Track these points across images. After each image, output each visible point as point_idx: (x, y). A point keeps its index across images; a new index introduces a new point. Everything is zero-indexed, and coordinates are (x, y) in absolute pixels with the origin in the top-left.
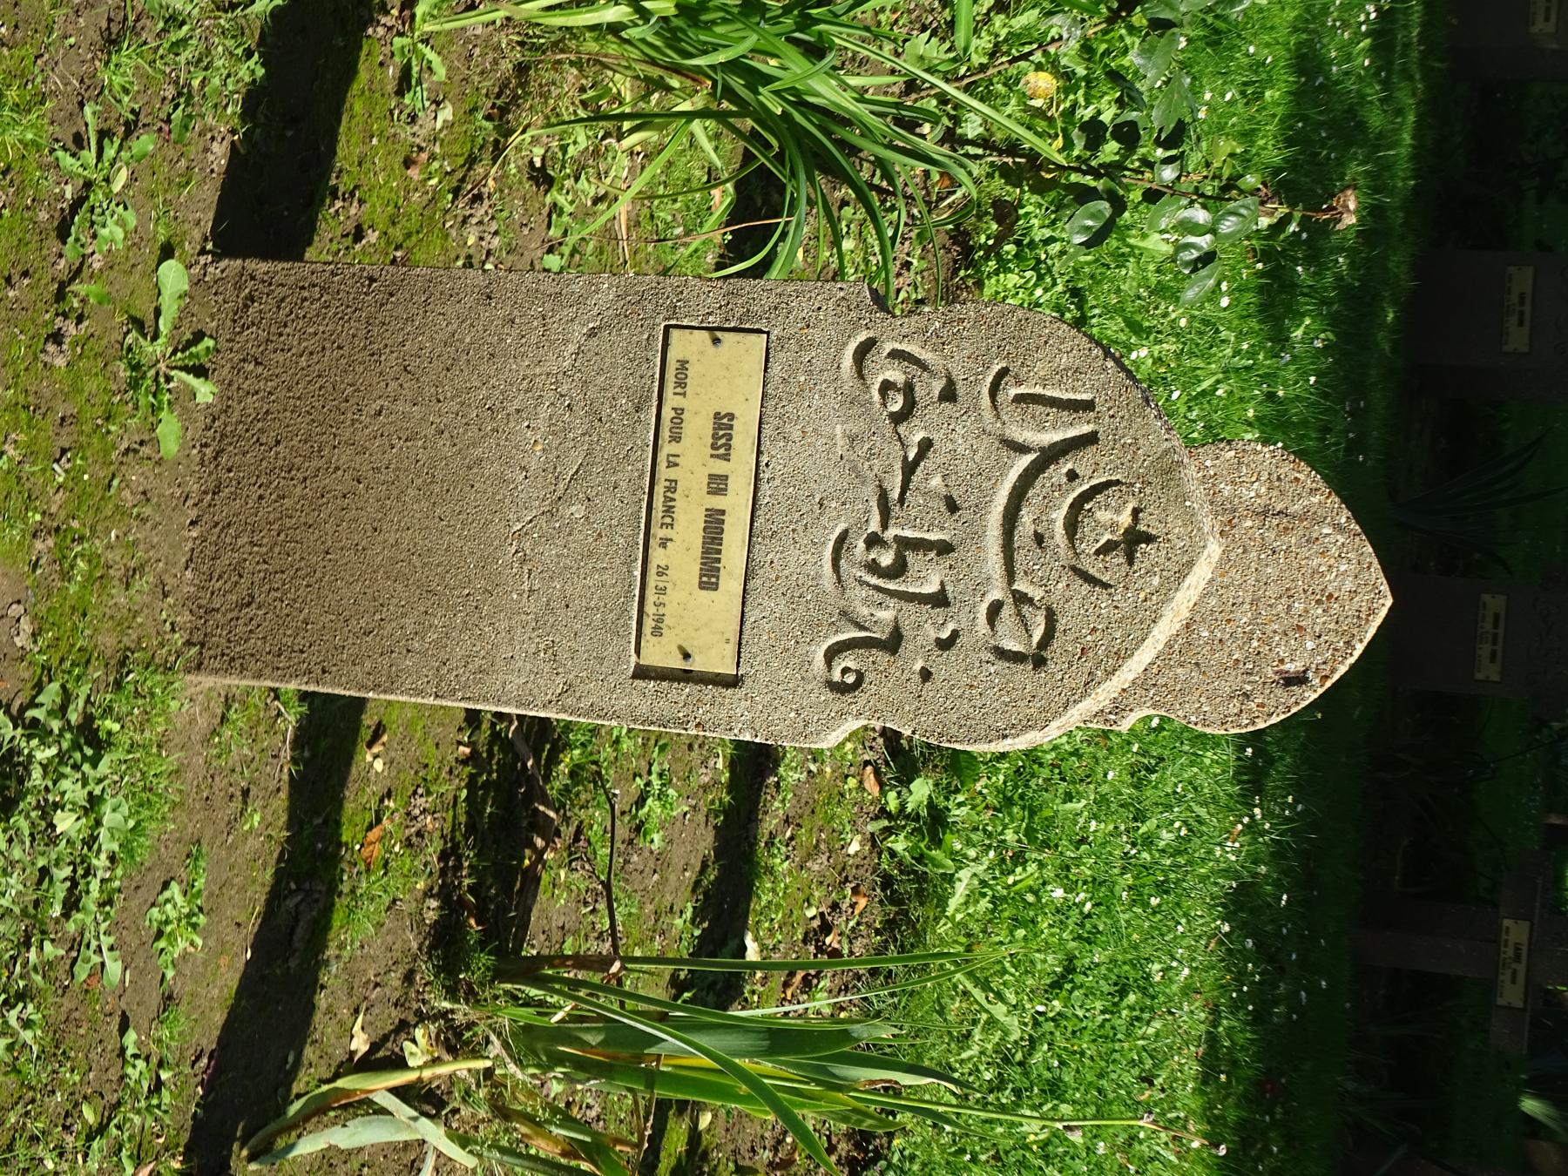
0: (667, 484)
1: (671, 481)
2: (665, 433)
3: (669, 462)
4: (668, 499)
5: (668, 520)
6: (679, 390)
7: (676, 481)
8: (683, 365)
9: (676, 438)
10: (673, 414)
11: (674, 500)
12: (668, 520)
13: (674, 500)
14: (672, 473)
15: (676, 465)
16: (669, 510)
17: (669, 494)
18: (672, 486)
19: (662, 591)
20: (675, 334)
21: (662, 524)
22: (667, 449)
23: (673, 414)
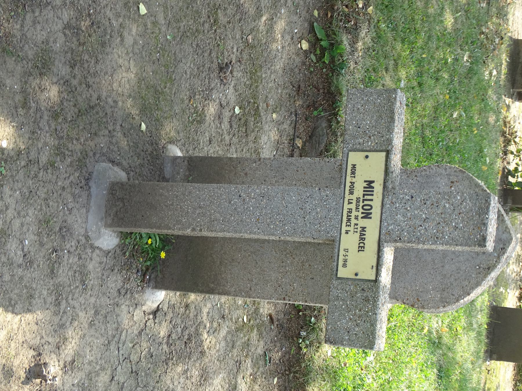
0: (348, 210)
1: (350, 209)
2: (347, 192)
3: (349, 202)
4: (348, 216)
5: (348, 224)
6: (352, 175)
7: (352, 209)
8: (354, 166)
9: (351, 193)
10: (350, 184)
11: (351, 216)
12: (348, 224)
13: (351, 216)
15: (352, 203)
16: (349, 220)
18: (350, 211)
19: (346, 250)
21: (346, 225)
22: (347, 197)
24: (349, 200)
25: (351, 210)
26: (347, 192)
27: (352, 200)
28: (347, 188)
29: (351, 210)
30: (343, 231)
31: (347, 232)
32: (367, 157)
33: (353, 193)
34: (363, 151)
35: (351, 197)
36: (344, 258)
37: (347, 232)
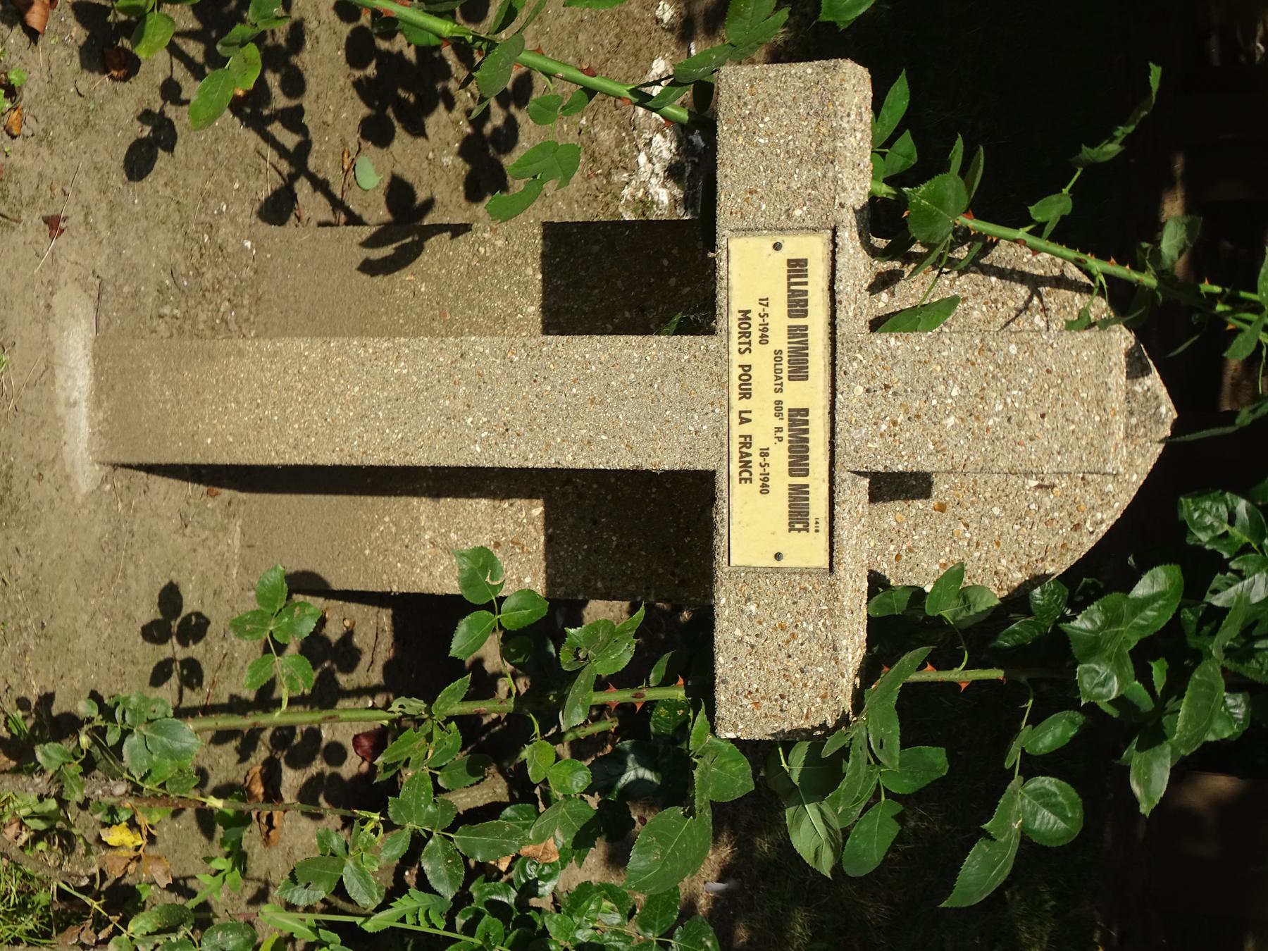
0: (742, 440)
1: (746, 437)
3: (741, 418)
4: (743, 455)
5: (745, 475)
7: (750, 437)
10: (740, 371)
12: (745, 475)
14: (746, 429)
15: (749, 420)
16: (746, 466)
17: (744, 450)
18: (746, 442)
21: (741, 480)
22: (738, 404)
23: (740, 371)
24: (741, 412)
25: (748, 439)
26: (735, 392)
27: (750, 412)
28: (735, 382)
29: (748, 439)
33: (750, 394)
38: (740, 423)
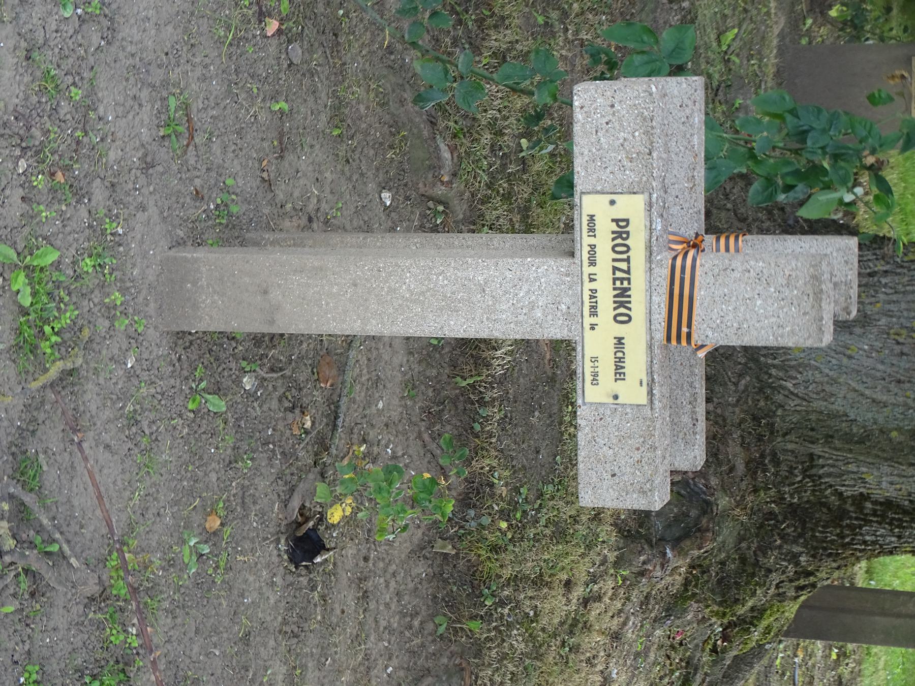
6: (591, 234)
9: (592, 263)
10: (589, 249)
14: (593, 285)
15: (595, 280)
19: (594, 360)
20: (584, 197)
22: (587, 270)
24: (590, 274)
26: (586, 262)
28: (585, 256)
30: (587, 326)
31: (592, 327)
32: (612, 202)
34: (602, 193)
35: (592, 270)
36: (592, 370)
37: (592, 327)
38: (590, 281)
